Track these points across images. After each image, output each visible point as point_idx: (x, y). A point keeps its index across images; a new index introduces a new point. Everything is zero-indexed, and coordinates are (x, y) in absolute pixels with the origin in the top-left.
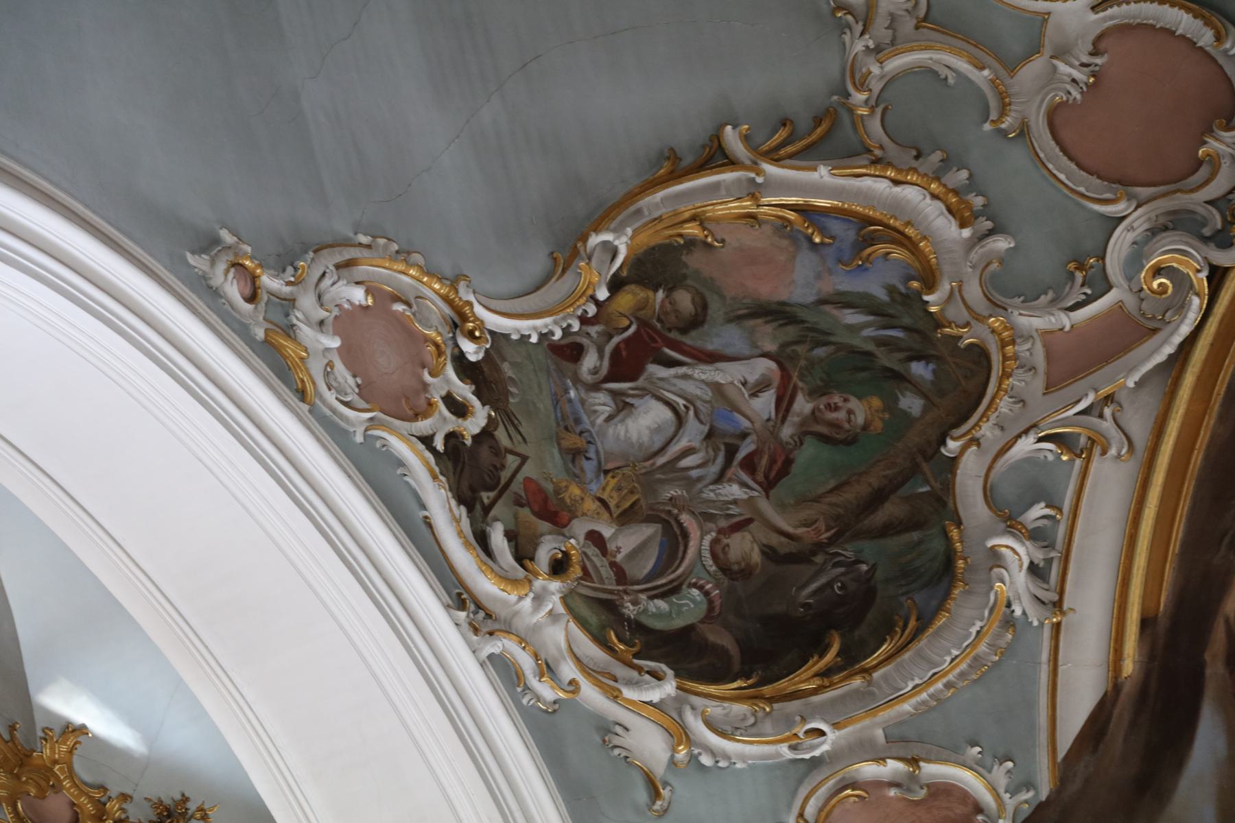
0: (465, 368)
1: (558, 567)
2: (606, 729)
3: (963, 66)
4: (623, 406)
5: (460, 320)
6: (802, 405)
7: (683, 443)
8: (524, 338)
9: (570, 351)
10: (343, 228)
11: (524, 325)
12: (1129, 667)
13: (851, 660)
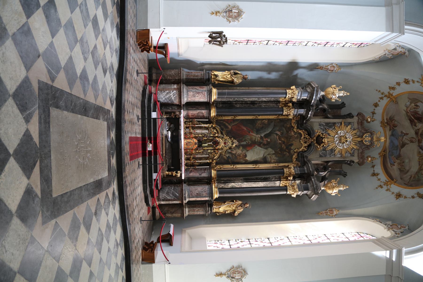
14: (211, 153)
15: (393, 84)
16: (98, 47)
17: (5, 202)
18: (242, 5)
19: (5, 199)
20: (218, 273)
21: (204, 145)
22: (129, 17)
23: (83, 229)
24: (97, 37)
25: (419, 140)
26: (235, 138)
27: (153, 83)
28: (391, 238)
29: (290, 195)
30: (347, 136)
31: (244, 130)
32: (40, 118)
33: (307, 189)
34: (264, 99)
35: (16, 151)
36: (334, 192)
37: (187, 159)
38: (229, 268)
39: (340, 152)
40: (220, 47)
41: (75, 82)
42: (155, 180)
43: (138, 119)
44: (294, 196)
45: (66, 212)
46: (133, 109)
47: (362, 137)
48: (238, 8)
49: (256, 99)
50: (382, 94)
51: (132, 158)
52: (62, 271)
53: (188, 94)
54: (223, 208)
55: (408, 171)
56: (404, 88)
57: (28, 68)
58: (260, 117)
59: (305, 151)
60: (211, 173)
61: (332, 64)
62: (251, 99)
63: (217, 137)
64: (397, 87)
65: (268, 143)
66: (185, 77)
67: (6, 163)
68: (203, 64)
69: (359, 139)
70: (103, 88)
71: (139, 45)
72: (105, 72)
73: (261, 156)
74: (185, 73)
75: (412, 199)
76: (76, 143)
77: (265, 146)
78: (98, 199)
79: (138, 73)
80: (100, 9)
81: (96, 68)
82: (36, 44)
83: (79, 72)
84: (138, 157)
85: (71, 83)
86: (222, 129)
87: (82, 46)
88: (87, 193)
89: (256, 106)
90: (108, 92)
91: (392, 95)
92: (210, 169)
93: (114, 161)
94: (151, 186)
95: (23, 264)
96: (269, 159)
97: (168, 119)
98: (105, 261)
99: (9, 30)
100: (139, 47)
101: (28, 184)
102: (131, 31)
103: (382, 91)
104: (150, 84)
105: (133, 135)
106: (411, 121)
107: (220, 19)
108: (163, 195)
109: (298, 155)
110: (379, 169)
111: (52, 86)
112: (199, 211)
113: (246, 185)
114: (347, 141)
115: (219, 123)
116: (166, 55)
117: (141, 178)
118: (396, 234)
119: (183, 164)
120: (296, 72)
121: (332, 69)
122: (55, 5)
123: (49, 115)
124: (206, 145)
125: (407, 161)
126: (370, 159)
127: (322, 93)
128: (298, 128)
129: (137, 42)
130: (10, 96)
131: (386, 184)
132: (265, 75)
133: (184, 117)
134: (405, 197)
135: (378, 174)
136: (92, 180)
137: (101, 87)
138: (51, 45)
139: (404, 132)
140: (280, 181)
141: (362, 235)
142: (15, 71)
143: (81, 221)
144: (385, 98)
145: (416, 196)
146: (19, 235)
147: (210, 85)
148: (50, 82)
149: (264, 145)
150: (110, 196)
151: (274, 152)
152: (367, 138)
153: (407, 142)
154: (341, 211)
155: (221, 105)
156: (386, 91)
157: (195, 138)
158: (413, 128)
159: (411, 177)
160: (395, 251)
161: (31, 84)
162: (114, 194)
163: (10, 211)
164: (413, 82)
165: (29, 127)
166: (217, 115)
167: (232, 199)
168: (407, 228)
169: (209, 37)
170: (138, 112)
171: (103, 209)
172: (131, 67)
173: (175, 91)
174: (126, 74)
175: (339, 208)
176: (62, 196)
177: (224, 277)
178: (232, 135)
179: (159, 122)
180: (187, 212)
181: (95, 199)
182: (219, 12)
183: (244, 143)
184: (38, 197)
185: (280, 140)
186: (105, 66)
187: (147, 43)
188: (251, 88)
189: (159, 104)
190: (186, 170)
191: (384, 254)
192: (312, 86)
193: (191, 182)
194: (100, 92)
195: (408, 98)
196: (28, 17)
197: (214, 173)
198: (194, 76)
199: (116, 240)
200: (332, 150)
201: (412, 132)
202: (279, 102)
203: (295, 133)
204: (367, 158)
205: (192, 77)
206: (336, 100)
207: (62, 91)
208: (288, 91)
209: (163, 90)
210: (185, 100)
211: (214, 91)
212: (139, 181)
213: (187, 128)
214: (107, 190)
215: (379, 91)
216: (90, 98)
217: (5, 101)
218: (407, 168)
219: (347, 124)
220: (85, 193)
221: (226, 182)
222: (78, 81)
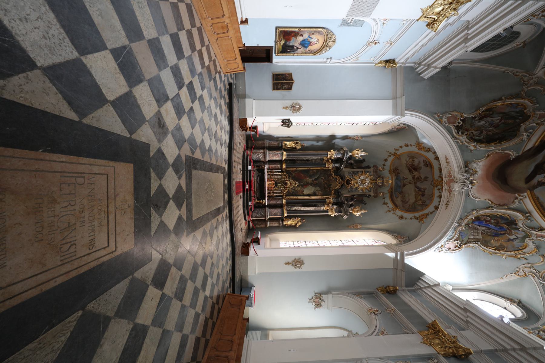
0: (461, 120)
1: (466, 135)
2: (467, 146)
3: (540, 88)
4: (479, 122)
5: (462, 116)
6: (503, 121)
7: (486, 124)
8: (469, 117)
9: (475, 117)
10: (451, 110)
11: (470, 116)
12: (536, 145)
13: (500, 142)
14: (283, 190)
15: (397, 147)
16: (217, 131)
17: (167, 225)
18: (301, 102)
19: (167, 224)
20: (287, 262)
21: (278, 185)
22: (235, 111)
23: (209, 238)
24: (217, 126)
25: (415, 182)
26: (296, 181)
27: (249, 149)
28: (396, 245)
29: (330, 215)
30: (366, 180)
31: (302, 176)
32: (186, 176)
33: (341, 212)
34: (314, 158)
35: (173, 196)
36: (358, 214)
37: (269, 193)
38: (293, 260)
39: (362, 189)
40: (288, 128)
41: (205, 153)
42: (250, 205)
43: (241, 171)
44: (333, 216)
45: (200, 228)
46: (238, 165)
47: (376, 180)
48: (299, 105)
49: (310, 158)
50: (390, 153)
51: (237, 194)
52: (197, 263)
53: (269, 156)
54: (289, 222)
55: (408, 202)
56: (405, 150)
57: (180, 149)
58: (312, 168)
59: (339, 189)
60: (282, 201)
61: (357, 135)
62: (306, 158)
63: (286, 180)
64: (400, 149)
65: (317, 184)
66: (267, 145)
67: (168, 203)
68: (278, 138)
69: (374, 182)
70: (220, 155)
71: (241, 127)
72: (222, 145)
73: (313, 191)
74: (267, 143)
75: (410, 220)
76: (206, 188)
78: (218, 219)
79: (240, 144)
80: (218, 109)
81: (217, 144)
82: (184, 135)
83: (207, 147)
84: (240, 193)
85: (203, 154)
86: (289, 176)
87: (209, 132)
88: (212, 216)
89: (309, 162)
90: (224, 157)
91: (397, 154)
92: (282, 199)
93: (227, 196)
94: (247, 209)
95: (176, 260)
96: (317, 193)
97: (257, 170)
98: (220, 256)
99: (169, 129)
100: (240, 128)
101: (180, 214)
102: (236, 119)
103: (390, 152)
104: (247, 150)
105: (238, 180)
106: (410, 170)
107: (288, 111)
108: (254, 214)
109: (335, 191)
110: (388, 200)
111: (193, 158)
112: (276, 224)
113: (303, 208)
114: (366, 183)
115: (287, 172)
116: (256, 132)
117: (242, 204)
118: (400, 242)
119: (266, 196)
120: (334, 141)
121: (357, 138)
122: (193, 111)
123: (191, 174)
124: (280, 185)
125: (407, 195)
126: (381, 194)
127: (350, 154)
128: (335, 175)
129: (239, 125)
130: (170, 166)
131: (393, 209)
132: (315, 143)
133: (267, 169)
134: (406, 219)
135: (387, 203)
136: (214, 208)
137: (219, 154)
138: (192, 134)
139: (405, 177)
140: (324, 206)
141: (377, 241)
142: (173, 152)
143: (208, 233)
144: (392, 156)
145: (413, 218)
146: (174, 244)
147: (282, 150)
148: (191, 155)
149: (314, 185)
150: (224, 217)
151: (320, 189)
152: (379, 181)
153: (407, 183)
154: (363, 226)
155: (288, 162)
156: (393, 151)
157: (274, 181)
158: (411, 175)
159: (410, 206)
160: (399, 253)
161: (181, 157)
162: (226, 215)
163: (170, 230)
164: (411, 145)
165: (180, 182)
166: (286, 168)
167: (295, 217)
168: (407, 238)
169: (282, 122)
170: (240, 167)
171: (220, 225)
172: (236, 141)
173: (262, 154)
174: (233, 145)
175: (361, 224)
176: (198, 219)
177: (290, 265)
178: (295, 179)
179: (252, 172)
180: (268, 224)
181: (216, 219)
182: (287, 107)
183: (302, 184)
184: (185, 221)
185: (324, 182)
186: (222, 142)
187: (245, 126)
188: (306, 151)
189: (252, 161)
190: (268, 200)
191: (391, 255)
192: (344, 150)
193: (271, 206)
194: (219, 158)
195: (408, 156)
196: (179, 120)
197: (284, 201)
198: (273, 144)
199: (227, 242)
200: (357, 188)
201: (410, 178)
202: (323, 159)
203: (333, 178)
204: (380, 193)
205: (272, 145)
206: (359, 158)
207: (198, 159)
208: (329, 153)
209: (255, 153)
210: (267, 159)
211: (285, 153)
212: (241, 206)
213: (269, 175)
214: (223, 213)
215: (388, 151)
216: (214, 162)
217: (168, 169)
218: (407, 200)
219: (366, 173)
220: (210, 216)
221: (291, 207)
222: (207, 153)
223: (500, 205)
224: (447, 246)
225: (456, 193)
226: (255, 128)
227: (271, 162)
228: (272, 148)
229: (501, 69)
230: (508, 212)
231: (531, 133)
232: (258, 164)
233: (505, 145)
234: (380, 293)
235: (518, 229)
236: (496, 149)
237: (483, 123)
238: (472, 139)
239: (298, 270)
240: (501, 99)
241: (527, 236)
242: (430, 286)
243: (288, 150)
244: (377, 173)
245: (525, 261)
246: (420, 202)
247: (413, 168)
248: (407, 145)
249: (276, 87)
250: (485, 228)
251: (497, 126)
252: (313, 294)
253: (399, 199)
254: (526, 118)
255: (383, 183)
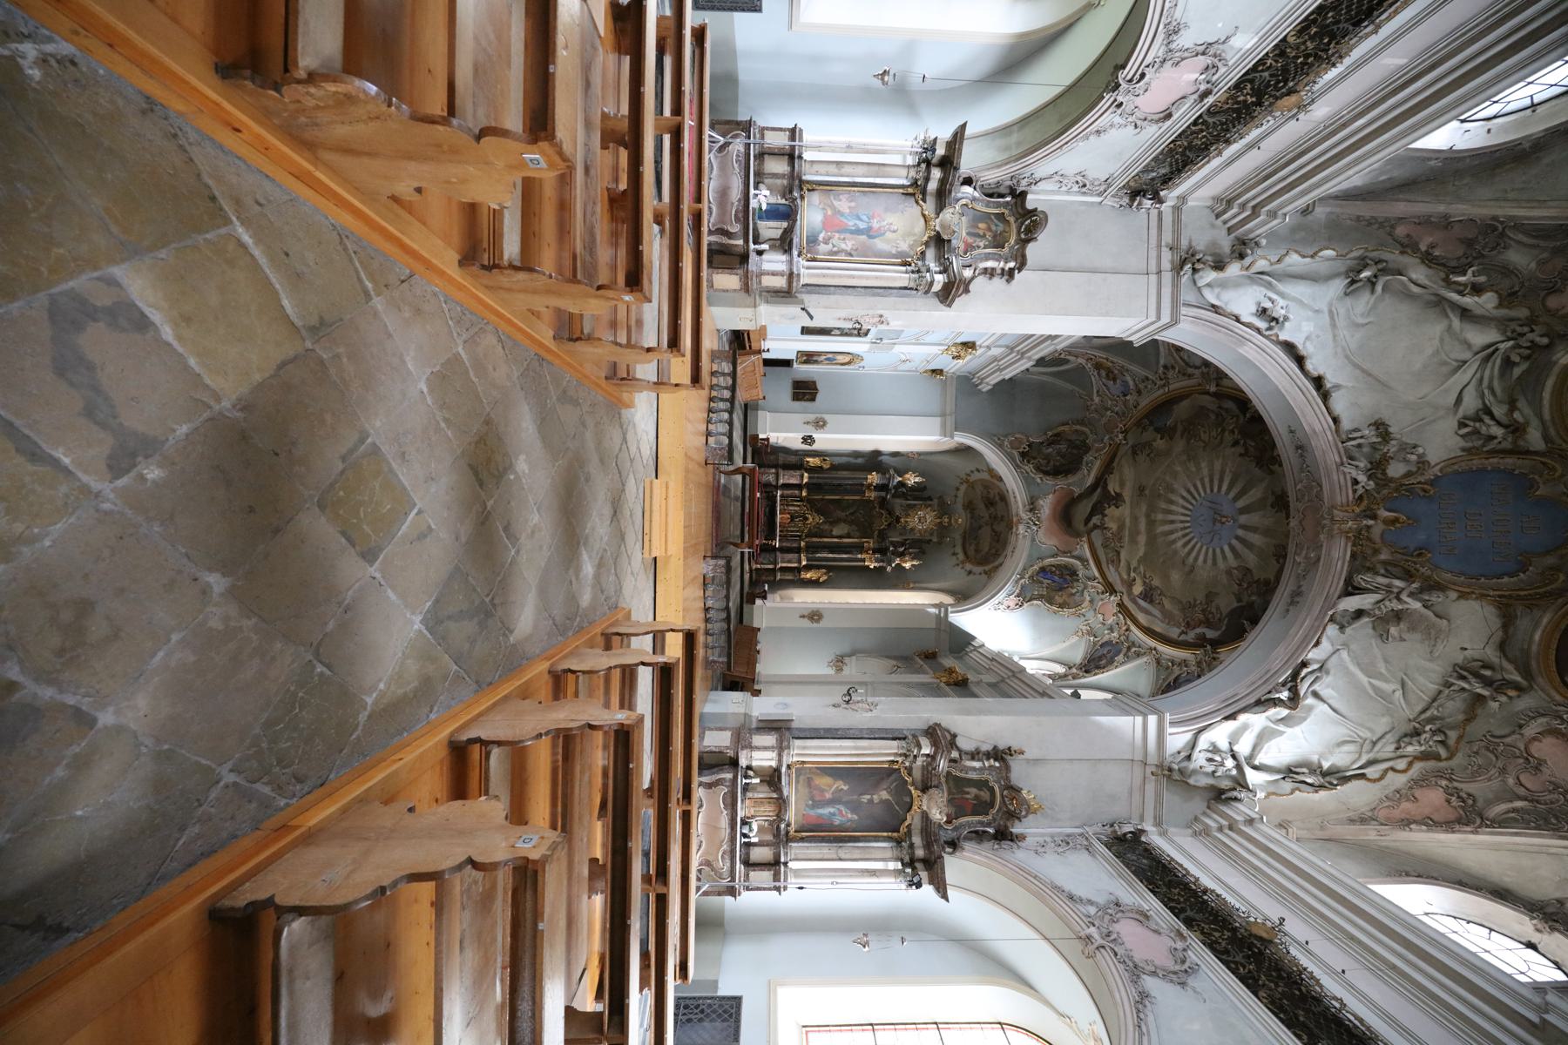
18: (826, 417)
29: (868, 567)
39: (920, 531)
69: (938, 521)
74: (782, 458)
77: (851, 523)
86: (811, 507)
92: (800, 540)
96: (852, 534)
106: (986, 506)
108: (761, 560)
110: (959, 549)
112: (789, 577)
113: (831, 555)
115: (808, 500)
120: (880, 458)
131: (963, 562)
132: (852, 460)
154: (917, 585)
156: (964, 477)
160: (943, 610)
167: (818, 567)
175: (915, 583)
178: (820, 512)
180: (778, 577)
191: (933, 610)
193: (783, 550)
197: (803, 544)
200: (912, 529)
210: (781, 482)
211: (806, 475)
219: (927, 507)
221: (813, 553)
223: (1065, 553)
224: (1006, 603)
225: (1021, 537)
226: (768, 439)
227: (786, 486)
228: (788, 467)
229: (1069, 387)
230: (1071, 560)
231: (1090, 466)
232: (769, 490)
233: (1072, 479)
234: (917, 659)
235: (1078, 581)
236: (1061, 483)
237: (1050, 450)
238: (1038, 469)
239: (815, 625)
240: (1068, 424)
241: (1085, 588)
242: (976, 649)
243: (811, 470)
244: (944, 509)
245: (1083, 619)
246: (993, 551)
247: (990, 503)
248: (978, 470)
249: (797, 397)
250: (1049, 582)
251: (1063, 456)
252: (833, 657)
253: (972, 548)
254: (1087, 449)
255: (950, 522)
